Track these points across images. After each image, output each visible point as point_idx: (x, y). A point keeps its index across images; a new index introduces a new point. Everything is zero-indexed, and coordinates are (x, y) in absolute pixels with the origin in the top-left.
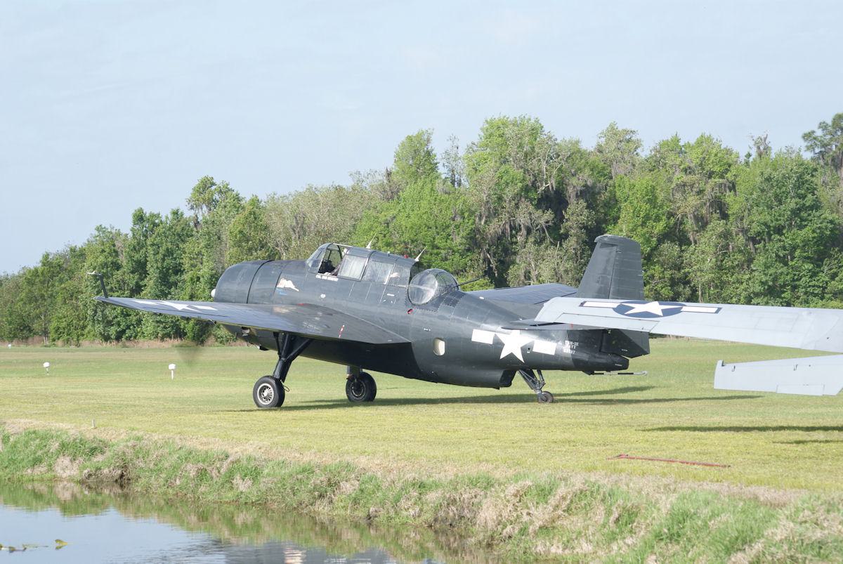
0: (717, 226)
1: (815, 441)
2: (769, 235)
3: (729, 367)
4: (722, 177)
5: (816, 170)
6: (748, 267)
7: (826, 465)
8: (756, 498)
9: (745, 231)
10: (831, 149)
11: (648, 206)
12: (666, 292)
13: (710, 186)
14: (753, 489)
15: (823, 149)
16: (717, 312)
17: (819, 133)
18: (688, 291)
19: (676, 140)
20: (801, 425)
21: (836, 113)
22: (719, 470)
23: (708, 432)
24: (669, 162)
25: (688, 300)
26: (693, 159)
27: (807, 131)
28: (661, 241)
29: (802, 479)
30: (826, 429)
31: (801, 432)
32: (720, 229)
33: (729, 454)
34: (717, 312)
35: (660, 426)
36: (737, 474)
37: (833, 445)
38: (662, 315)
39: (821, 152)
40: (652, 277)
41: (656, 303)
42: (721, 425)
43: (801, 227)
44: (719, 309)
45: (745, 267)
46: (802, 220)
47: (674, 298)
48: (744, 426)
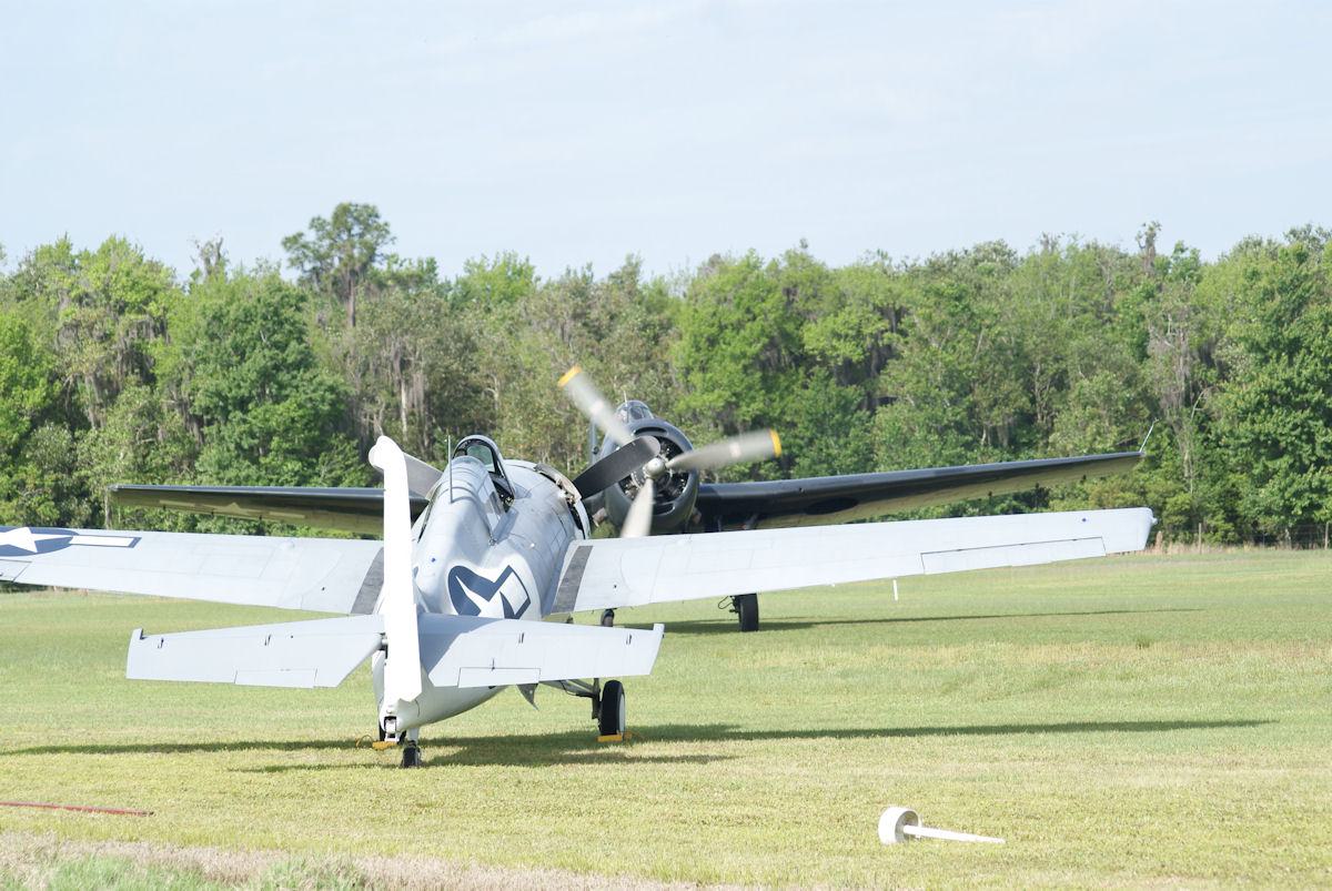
0: (134, 396)
1: (301, 767)
2: (225, 412)
3: (153, 640)
4: (141, 311)
5: (303, 299)
6: (191, 466)
7: (319, 809)
8: (198, 869)
9: (183, 405)
10: (331, 265)
11: (14, 361)
12: (47, 510)
13: (121, 329)
14: (191, 852)
15: (318, 264)
16: (132, 545)
17: (311, 236)
18: (85, 509)
19: (65, 246)
20: (277, 740)
21: (338, 203)
22: (134, 821)
23: (116, 755)
24: (51, 287)
25: (86, 525)
26: (90, 281)
27: (291, 233)
28: (36, 423)
29: (276, 834)
30: (319, 745)
31: (277, 752)
32: (140, 403)
33: (151, 791)
34: (132, 545)
35: (32, 746)
36: (164, 827)
37: (332, 773)
38: (35, 551)
39: (314, 268)
40: (22, 485)
41: (26, 530)
42: (139, 742)
43: (277, 400)
44: (137, 540)
45: (185, 467)
46: (281, 386)
47: (62, 522)
48: (179, 743)
